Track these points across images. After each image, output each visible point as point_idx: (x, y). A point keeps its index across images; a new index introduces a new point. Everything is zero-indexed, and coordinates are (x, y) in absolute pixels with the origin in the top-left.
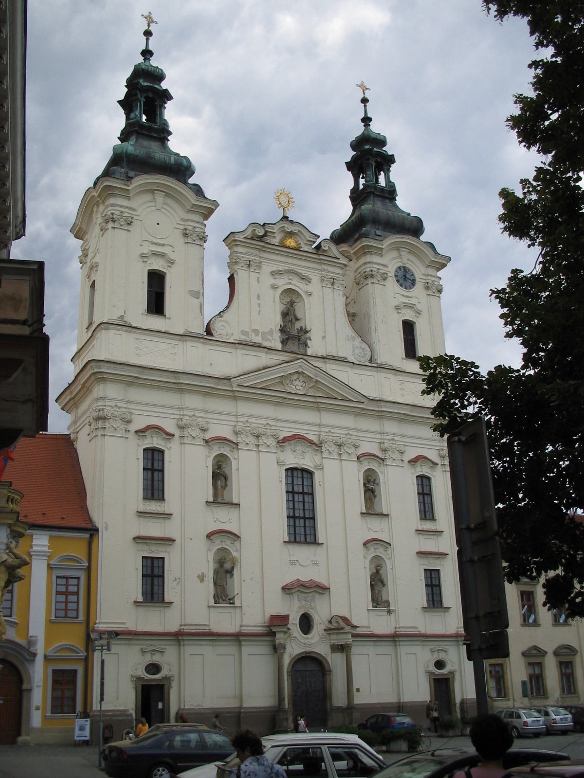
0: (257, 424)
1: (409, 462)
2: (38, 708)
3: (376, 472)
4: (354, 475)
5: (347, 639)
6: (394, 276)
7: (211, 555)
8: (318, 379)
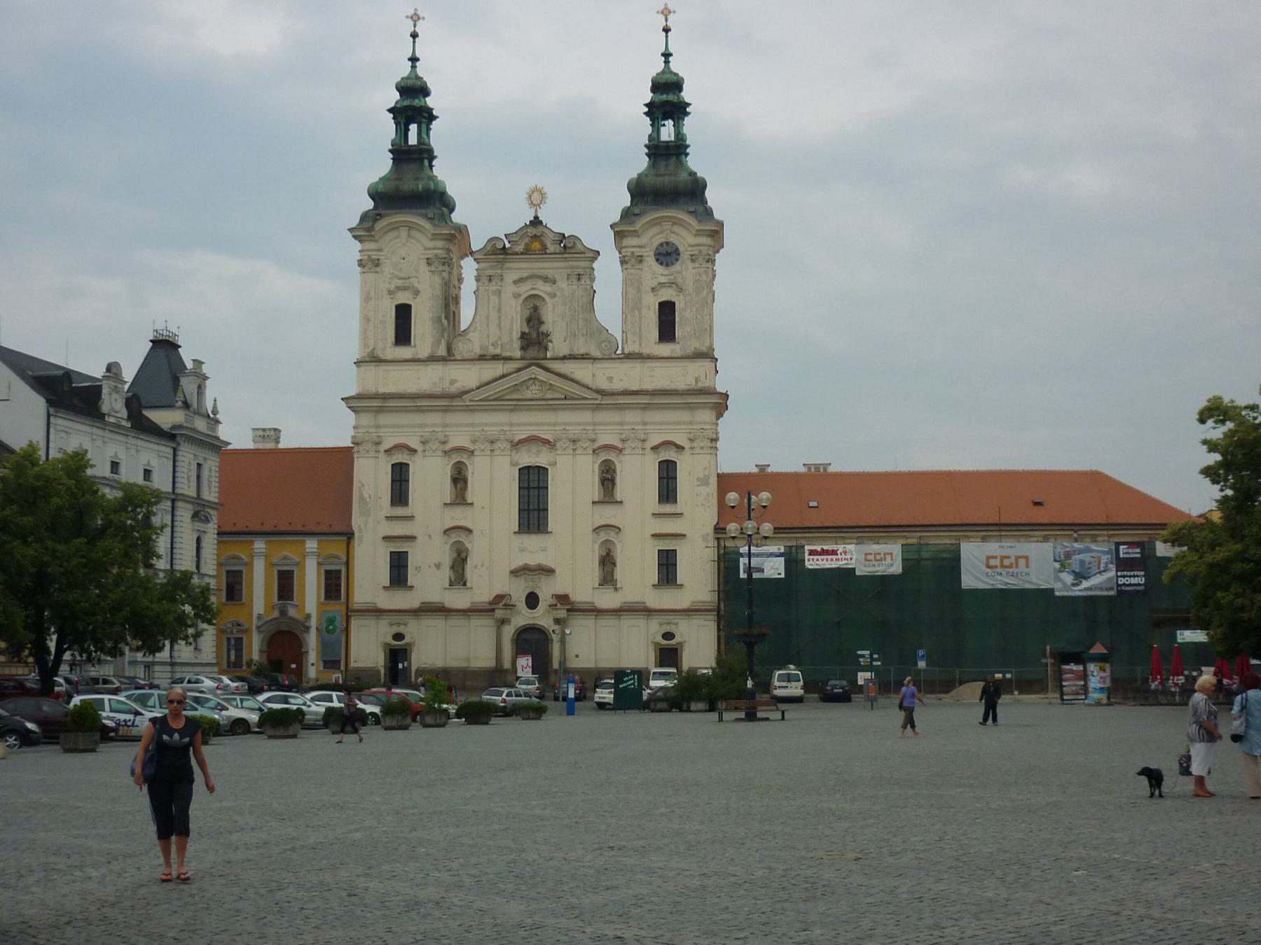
0: (492, 431)
1: (652, 448)
2: (313, 665)
3: (613, 462)
4: (588, 469)
5: (562, 614)
6: (653, 256)
7: (448, 547)
8: (551, 382)
